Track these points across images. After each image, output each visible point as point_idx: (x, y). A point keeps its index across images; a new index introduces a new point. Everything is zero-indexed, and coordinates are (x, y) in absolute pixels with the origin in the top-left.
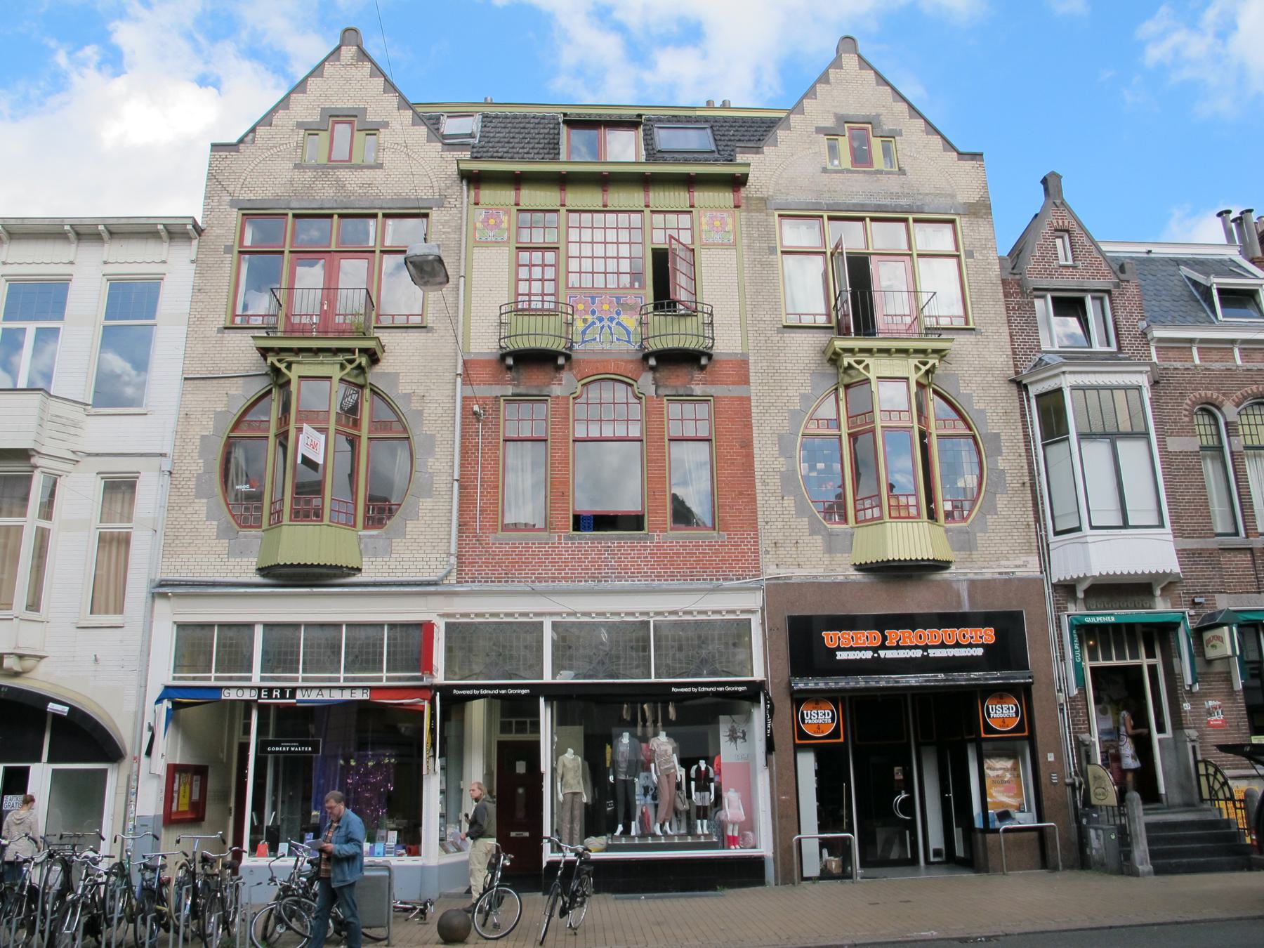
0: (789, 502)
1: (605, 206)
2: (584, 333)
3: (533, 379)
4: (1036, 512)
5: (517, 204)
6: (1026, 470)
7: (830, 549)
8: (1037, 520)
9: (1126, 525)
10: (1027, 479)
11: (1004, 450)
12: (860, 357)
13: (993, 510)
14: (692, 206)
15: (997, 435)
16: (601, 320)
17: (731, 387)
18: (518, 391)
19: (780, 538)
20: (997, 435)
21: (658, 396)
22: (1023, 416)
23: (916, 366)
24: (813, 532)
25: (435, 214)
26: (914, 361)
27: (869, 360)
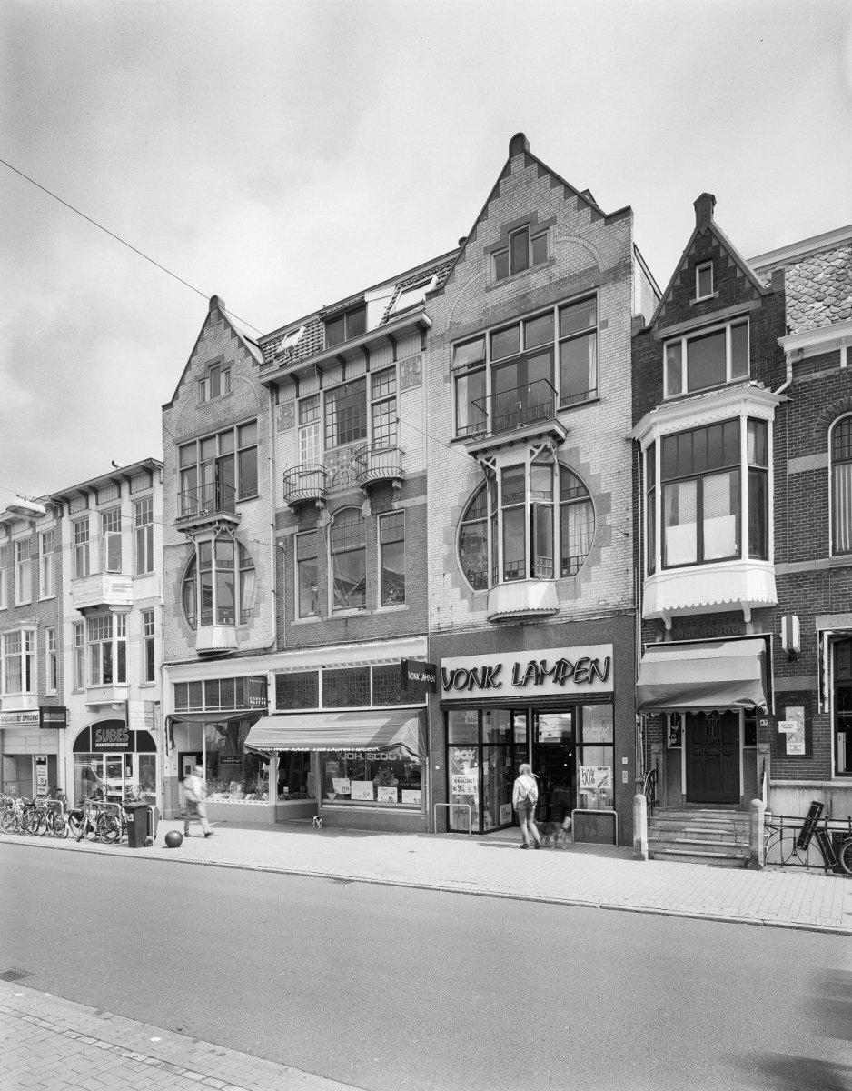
0: (449, 576)
1: (344, 380)
2: (333, 480)
3: (309, 518)
4: (635, 558)
5: (297, 397)
6: (631, 523)
7: (472, 609)
8: (635, 565)
9: (701, 560)
10: (631, 531)
11: (614, 507)
12: (488, 456)
13: (598, 560)
14: (395, 360)
15: (609, 495)
16: (342, 467)
17: (415, 499)
18: (303, 527)
19: (441, 605)
20: (609, 495)
21: (372, 515)
22: (634, 471)
23: (531, 451)
24: (463, 597)
25: (260, 419)
26: (530, 447)
27: (497, 457)
